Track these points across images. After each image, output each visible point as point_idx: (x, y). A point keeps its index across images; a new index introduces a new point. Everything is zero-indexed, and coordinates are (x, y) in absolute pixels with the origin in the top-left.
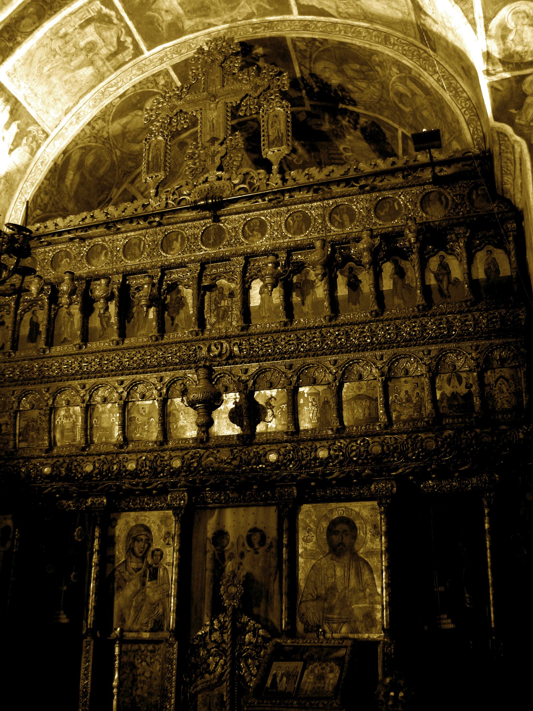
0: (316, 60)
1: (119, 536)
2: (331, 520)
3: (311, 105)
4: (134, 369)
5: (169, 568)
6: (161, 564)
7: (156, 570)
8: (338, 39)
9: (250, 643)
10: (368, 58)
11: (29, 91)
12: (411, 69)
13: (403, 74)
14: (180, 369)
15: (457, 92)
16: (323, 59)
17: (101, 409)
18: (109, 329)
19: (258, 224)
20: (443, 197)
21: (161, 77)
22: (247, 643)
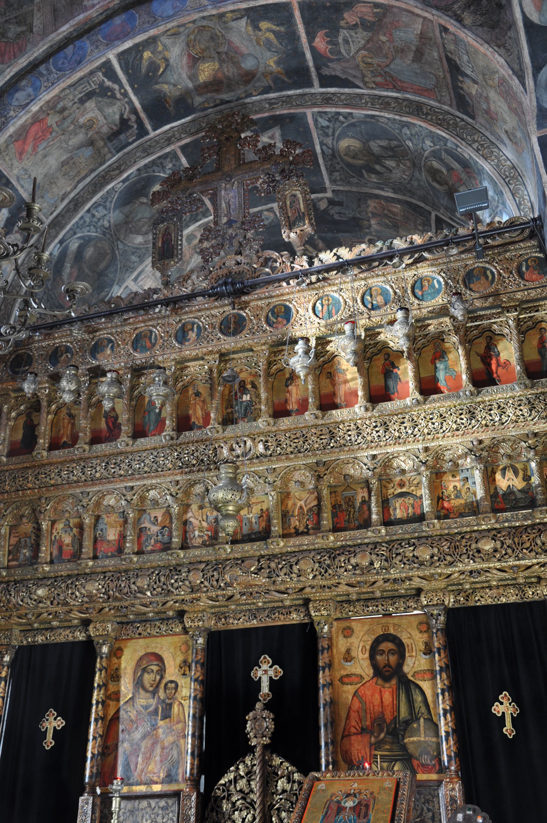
0: (339, 138)
1: (125, 668)
2: (373, 637)
3: (333, 191)
4: (146, 472)
5: (186, 703)
6: (176, 699)
7: (170, 705)
9: (284, 791)
10: (397, 131)
11: (22, 172)
12: (447, 140)
13: (438, 147)
14: (198, 471)
15: (499, 160)
16: (348, 136)
17: (106, 520)
18: (116, 430)
19: (283, 310)
20: (488, 272)
21: (169, 159)
22: (280, 791)
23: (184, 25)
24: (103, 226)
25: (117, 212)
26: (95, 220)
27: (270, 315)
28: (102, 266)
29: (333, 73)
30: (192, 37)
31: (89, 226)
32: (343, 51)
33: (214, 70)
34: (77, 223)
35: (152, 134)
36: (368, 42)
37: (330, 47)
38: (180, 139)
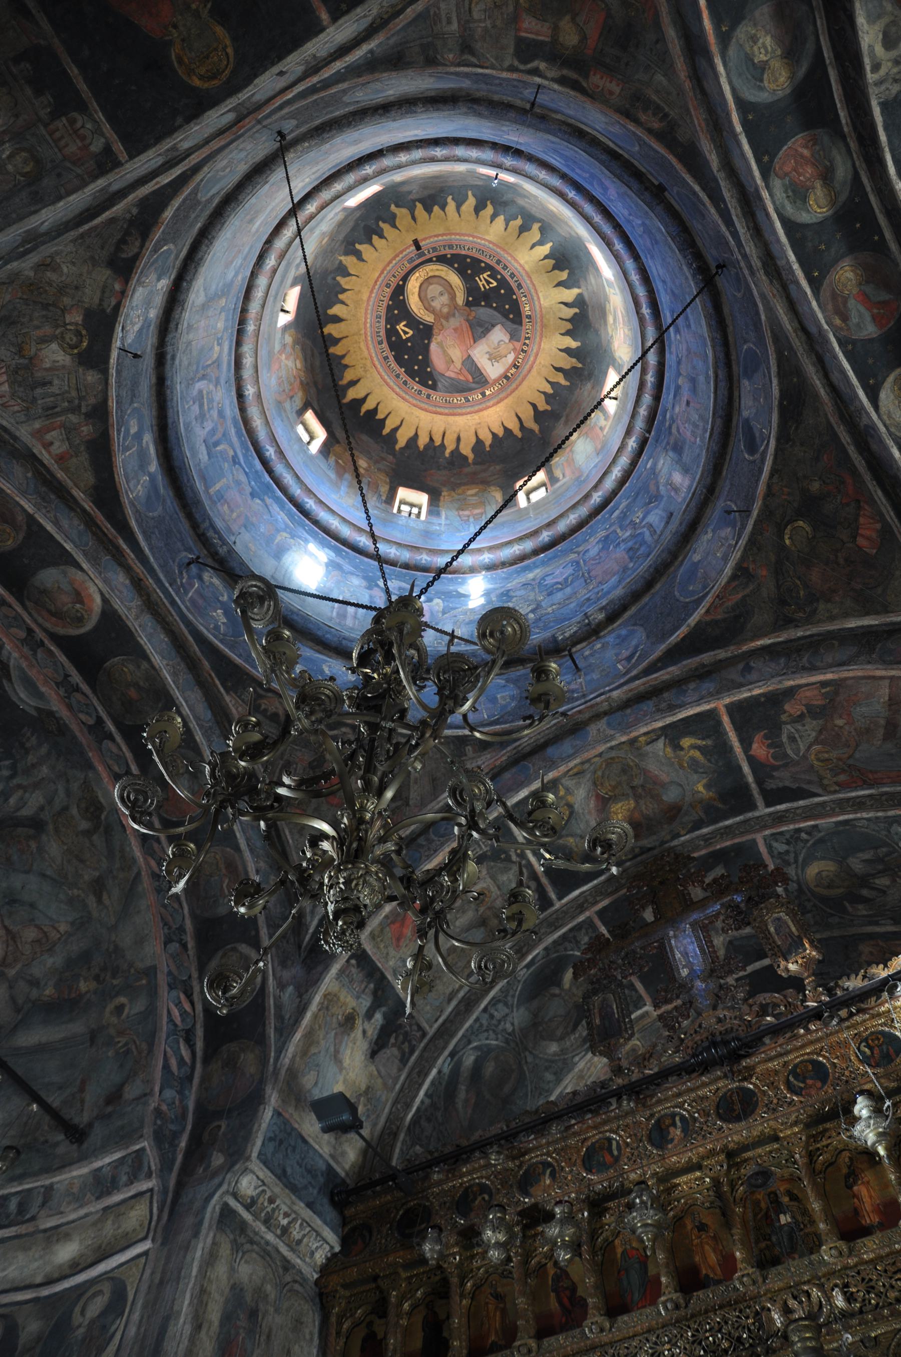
0: (806, 863)
8: (834, 820)
10: (884, 833)
16: (817, 859)
21: (583, 931)
23: (588, 761)
24: (505, 1030)
25: (522, 1010)
26: (494, 1022)
27: (791, 1078)
28: (507, 1089)
29: (781, 785)
30: (599, 773)
31: (487, 1031)
32: (789, 752)
33: (629, 810)
34: (471, 1026)
35: (558, 905)
36: (820, 732)
37: (772, 751)
38: (596, 903)
